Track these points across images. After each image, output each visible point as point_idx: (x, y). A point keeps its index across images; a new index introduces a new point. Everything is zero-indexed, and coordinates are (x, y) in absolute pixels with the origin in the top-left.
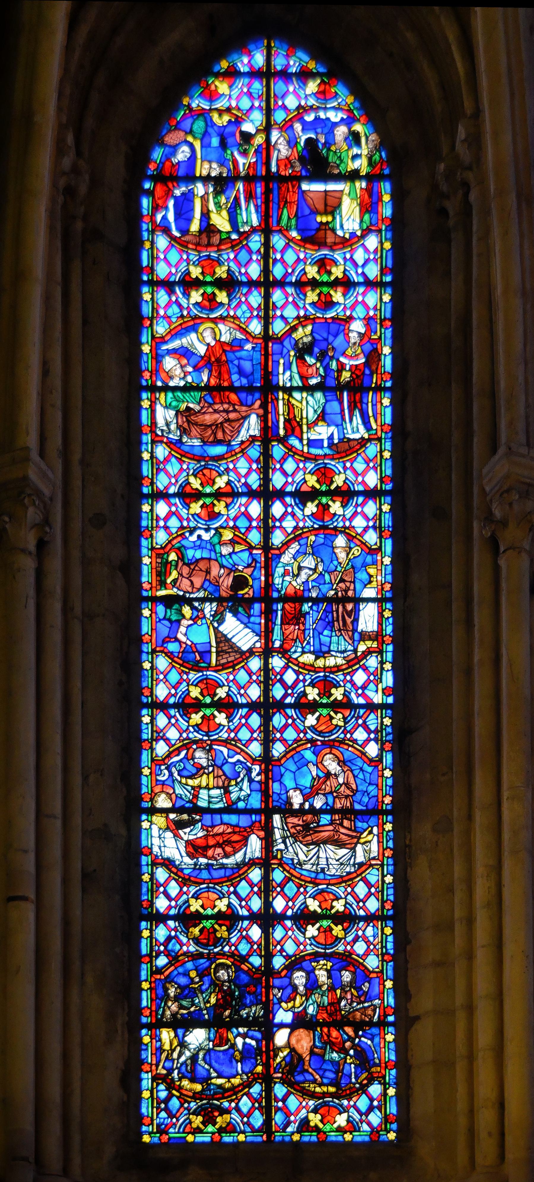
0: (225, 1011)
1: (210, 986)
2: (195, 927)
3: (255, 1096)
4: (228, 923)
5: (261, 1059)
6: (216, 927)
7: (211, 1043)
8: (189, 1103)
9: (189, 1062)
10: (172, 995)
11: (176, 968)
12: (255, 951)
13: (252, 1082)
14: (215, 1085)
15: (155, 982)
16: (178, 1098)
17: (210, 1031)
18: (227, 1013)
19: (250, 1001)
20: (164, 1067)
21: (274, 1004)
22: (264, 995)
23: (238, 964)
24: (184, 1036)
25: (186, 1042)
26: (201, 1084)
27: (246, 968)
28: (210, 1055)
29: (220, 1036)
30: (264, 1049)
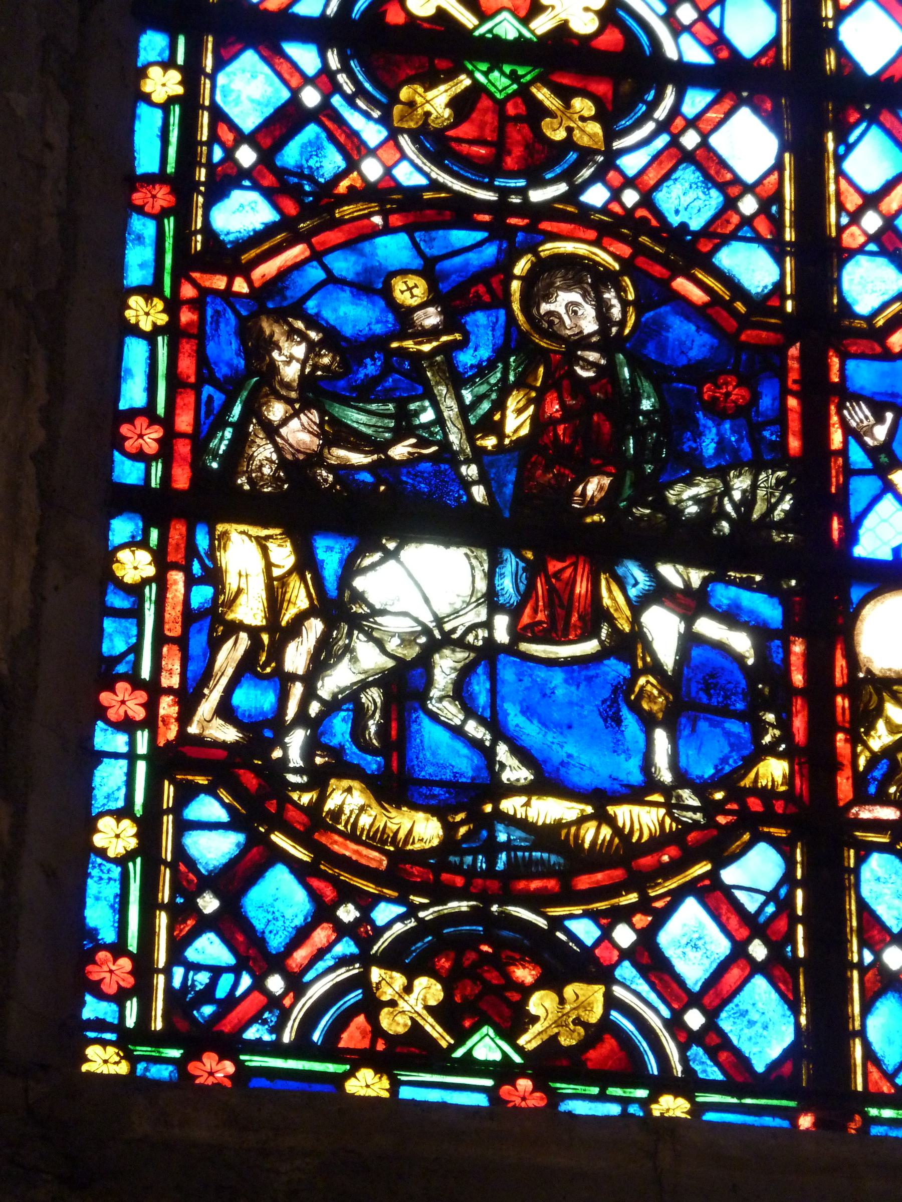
0: (584, 478)
1: (500, 355)
2: (430, 81)
3: (751, 903)
4: (602, 88)
5: (784, 724)
6: (543, 95)
7: (501, 622)
8: (366, 904)
9: (373, 697)
10: (291, 372)
11: (317, 256)
12: (747, 221)
13: (732, 832)
14: (523, 824)
15: (197, 304)
16: (299, 870)
17: (495, 562)
18: (594, 486)
19: (722, 444)
20: (226, 711)
21: (849, 472)
22: (794, 423)
23: (658, 270)
24: (349, 569)
25: (359, 597)
26: (439, 811)
27: (697, 295)
28: (493, 677)
29: (551, 591)
30: (798, 679)
